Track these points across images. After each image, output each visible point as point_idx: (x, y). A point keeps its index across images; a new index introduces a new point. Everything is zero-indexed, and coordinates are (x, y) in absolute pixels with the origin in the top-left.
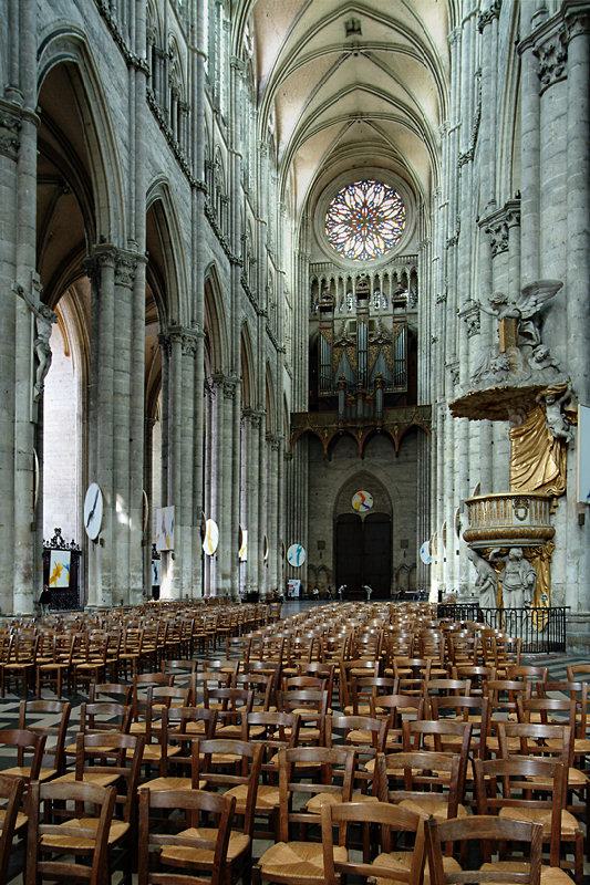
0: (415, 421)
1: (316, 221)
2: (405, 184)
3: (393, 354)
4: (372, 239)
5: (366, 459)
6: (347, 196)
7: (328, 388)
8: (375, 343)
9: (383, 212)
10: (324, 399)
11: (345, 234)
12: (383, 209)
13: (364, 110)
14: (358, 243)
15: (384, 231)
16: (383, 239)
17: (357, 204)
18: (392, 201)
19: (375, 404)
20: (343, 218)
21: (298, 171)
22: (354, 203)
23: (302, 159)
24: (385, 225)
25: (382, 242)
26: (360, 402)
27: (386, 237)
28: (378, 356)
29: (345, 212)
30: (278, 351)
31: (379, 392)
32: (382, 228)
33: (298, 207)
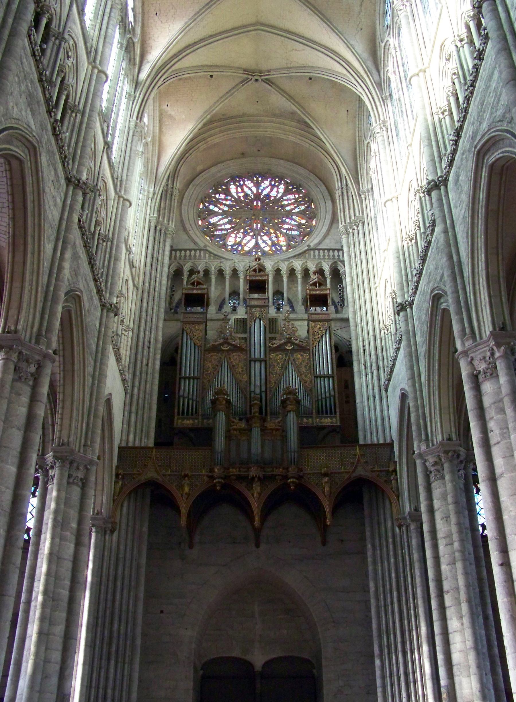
0: (361, 472)
1: (184, 208)
2: (312, 177)
3: (311, 365)
4: (268, 234)
5: (263, 547)
6: (233, 188)
7: (193, 413)
8: (279, 349)
9: (283, 207)
10: (183, 432)
11: (228, 226)
12: (285, 203)
13: (264, 66)
14: (248, 238)
15: (286, 226)
16: (285, 235)
17: (246, 196)
18: (297, 196)
19: (284, 438)
20: (226, 209)
21: (164, 130)
22: (241, 195)
23: (171, 116)
24: (287, 220)
25: (282, 239)
26: (256, 432)
27: (289, 232)
28: (285, 367)
29: (228, 203)
30: (103, 306)
31: (292, 418)
32: (284, 222)
33: (162, 169)
